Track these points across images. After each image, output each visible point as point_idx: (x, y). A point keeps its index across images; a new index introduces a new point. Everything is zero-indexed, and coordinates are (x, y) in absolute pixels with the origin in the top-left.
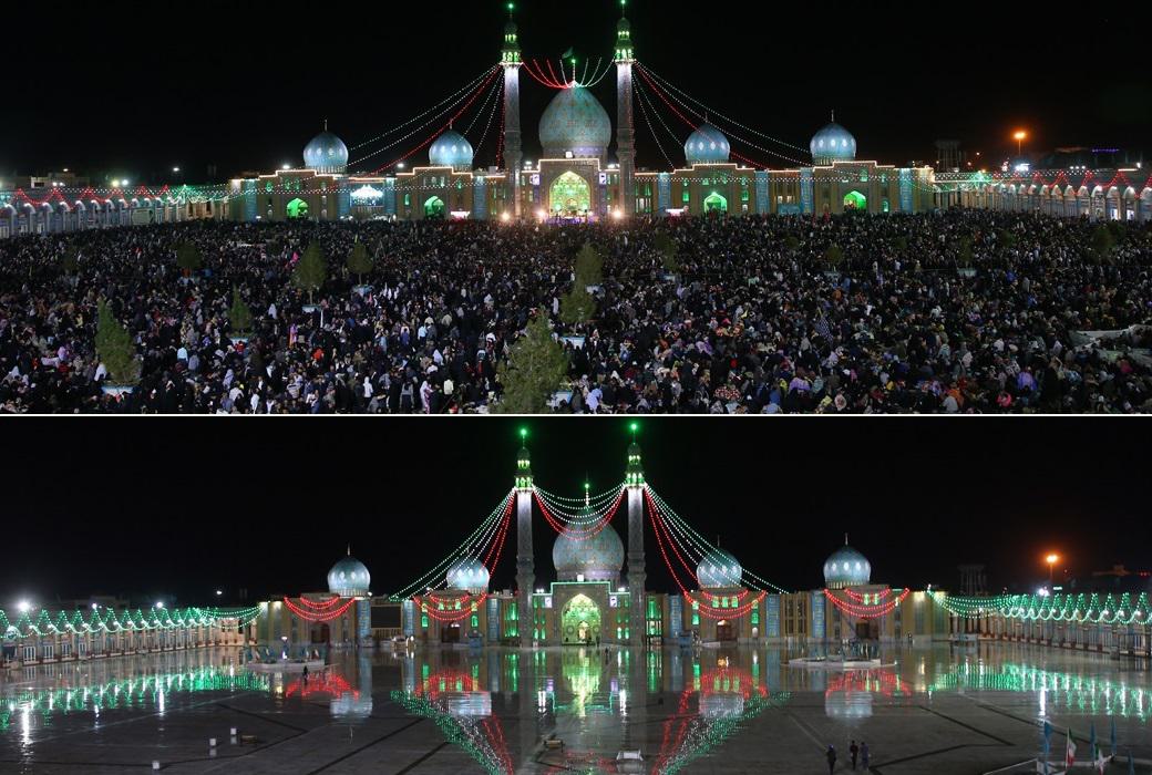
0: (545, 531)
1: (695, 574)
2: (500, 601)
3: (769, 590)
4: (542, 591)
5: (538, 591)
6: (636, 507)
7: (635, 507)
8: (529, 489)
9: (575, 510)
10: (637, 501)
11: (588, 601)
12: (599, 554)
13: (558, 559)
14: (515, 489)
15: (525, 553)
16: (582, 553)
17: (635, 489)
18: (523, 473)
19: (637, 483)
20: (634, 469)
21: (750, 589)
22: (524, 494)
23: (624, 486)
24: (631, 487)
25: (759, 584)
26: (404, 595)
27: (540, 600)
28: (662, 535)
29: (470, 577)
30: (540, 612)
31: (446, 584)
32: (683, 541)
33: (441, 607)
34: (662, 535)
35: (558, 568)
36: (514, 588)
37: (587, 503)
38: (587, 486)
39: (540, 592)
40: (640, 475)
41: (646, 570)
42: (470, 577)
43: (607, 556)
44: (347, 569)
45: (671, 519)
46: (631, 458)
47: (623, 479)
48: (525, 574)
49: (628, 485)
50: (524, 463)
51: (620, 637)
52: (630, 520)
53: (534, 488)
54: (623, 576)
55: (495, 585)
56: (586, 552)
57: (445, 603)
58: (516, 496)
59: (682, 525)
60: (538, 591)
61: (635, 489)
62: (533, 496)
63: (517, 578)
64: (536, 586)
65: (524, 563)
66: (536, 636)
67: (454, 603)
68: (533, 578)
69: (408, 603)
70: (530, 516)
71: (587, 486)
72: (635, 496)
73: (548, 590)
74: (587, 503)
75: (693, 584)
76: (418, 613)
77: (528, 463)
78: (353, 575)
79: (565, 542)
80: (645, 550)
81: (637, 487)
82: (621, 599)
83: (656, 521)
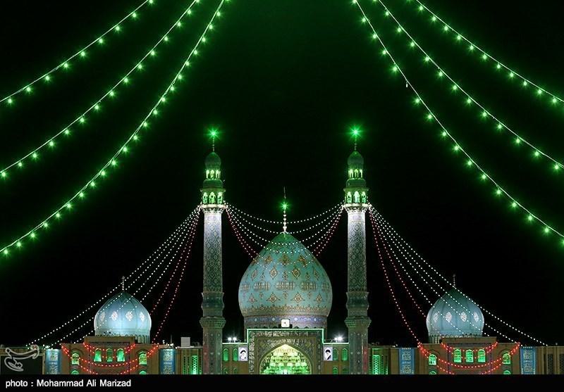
0: (238, 257)
1: (484, 313)
2: (178, 354)
3: (526, 342)
4: (235, 339)
5: (230, 339)
6: (358, 234)
7: (357, 234)
9: (271, 234)
10: (359, 226)
11: (293, 353)
12: (304, 294)
13: (245, 300)
15: (212, 289)
16: (282, 292)
18: (213, 186)
19: (361, 202)
20: (356, 185)
21: (501, 340)
24: (352, 208)
25: (516, 337)
27: (233, 351)
28: (392, 274)
32: (416, 277)
34: (392, 274)
35: (244, 315)
36: (197, 338)
37: (285, 228)
38: (285, 206)
39: (233, 340)
40: (364, 194)
41: (370, 314)
42: (126, 320)
43: (315, 295)
45: (403, 251)
46: (351, 172)
47: (341, 199)
48: (212, 320)
49: (205, 206)
50: (213, 173)
52: (350, 250)
54: (335, 321)
55: (164, 331)
57: (103, 354)
58: (202, 215)
59: (413, 255)
60: (230, 339)
61: (356, 214)
63: (201, 321)
64: (226, 332)
65: (212, 302)
67: (116, 354)
68: (223, 322)
70: (220, 240)
71: (285, 206)
72: (356, 220)
73: (242, 338)
74: (285, 228)
75: (423, 335)
77: (218, 172)
79: (258, 279)
80: (369, 287)
81: (361, 208)
82: (336, 351)
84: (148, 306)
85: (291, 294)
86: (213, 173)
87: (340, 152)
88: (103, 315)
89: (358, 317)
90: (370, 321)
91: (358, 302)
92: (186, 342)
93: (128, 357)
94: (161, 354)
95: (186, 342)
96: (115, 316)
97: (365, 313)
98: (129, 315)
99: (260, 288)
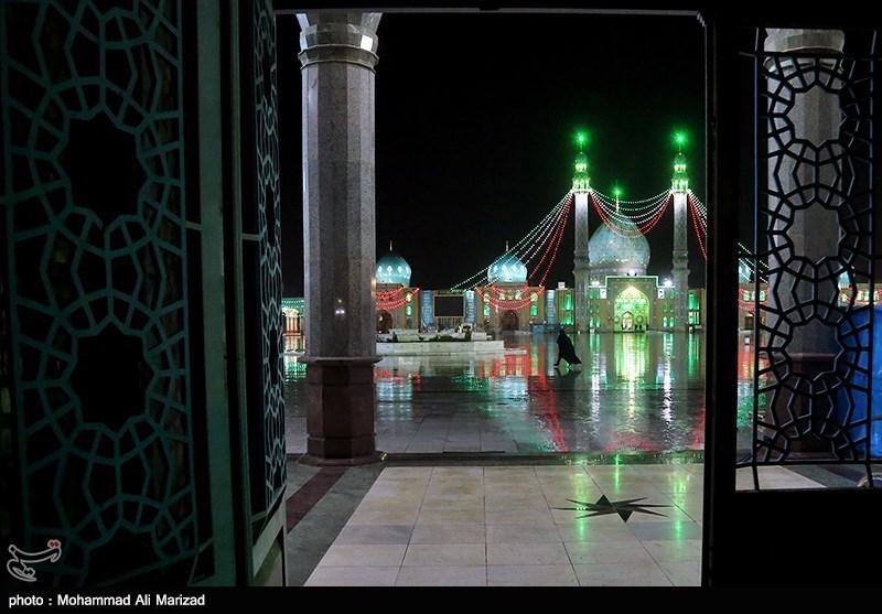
2: (557, 294)
8: (587, 190)
14: (572, 191)
17: (680, 194)
18: (581, 175)
22: (581, 193)
23: (671, 192)
26: (466, 286)
27: (597, 291)
29: (510, 271)
30: (596, 302)
31: (486, 274)
33: (502, 297)
36: (570, 284)
41: (688, 267)
44: (395, 264)
46: (676, 167)
51: (665, 325)
52: (676, 222)
53: (591, 190)
55: (533, 281)
56: (619, 247)
58: (574, 197)
60: (593, 283)
61: (680, 194)
62: (589, 196)
66: (591, 325)
69: (469, 294)
72: (680, 202)
76: (479, 300)
78: (400, 269)
79: (603, 242)
83: (698, 225)
84: (523, 261)
85: (628, 253)
86: (581, 166)
87: (669, 154)
88: (496, 268)
89: (683, 269)
90: (689, 272)
91: (682, 258)
92: (562, 286)
93: (523, 296)
94: (546, 294)
95: (562, 286)
96: (504, 267)
97: (686, 266)
98: (514, 267)
99: (605, 250)
